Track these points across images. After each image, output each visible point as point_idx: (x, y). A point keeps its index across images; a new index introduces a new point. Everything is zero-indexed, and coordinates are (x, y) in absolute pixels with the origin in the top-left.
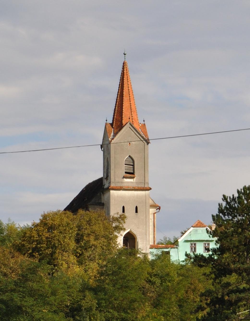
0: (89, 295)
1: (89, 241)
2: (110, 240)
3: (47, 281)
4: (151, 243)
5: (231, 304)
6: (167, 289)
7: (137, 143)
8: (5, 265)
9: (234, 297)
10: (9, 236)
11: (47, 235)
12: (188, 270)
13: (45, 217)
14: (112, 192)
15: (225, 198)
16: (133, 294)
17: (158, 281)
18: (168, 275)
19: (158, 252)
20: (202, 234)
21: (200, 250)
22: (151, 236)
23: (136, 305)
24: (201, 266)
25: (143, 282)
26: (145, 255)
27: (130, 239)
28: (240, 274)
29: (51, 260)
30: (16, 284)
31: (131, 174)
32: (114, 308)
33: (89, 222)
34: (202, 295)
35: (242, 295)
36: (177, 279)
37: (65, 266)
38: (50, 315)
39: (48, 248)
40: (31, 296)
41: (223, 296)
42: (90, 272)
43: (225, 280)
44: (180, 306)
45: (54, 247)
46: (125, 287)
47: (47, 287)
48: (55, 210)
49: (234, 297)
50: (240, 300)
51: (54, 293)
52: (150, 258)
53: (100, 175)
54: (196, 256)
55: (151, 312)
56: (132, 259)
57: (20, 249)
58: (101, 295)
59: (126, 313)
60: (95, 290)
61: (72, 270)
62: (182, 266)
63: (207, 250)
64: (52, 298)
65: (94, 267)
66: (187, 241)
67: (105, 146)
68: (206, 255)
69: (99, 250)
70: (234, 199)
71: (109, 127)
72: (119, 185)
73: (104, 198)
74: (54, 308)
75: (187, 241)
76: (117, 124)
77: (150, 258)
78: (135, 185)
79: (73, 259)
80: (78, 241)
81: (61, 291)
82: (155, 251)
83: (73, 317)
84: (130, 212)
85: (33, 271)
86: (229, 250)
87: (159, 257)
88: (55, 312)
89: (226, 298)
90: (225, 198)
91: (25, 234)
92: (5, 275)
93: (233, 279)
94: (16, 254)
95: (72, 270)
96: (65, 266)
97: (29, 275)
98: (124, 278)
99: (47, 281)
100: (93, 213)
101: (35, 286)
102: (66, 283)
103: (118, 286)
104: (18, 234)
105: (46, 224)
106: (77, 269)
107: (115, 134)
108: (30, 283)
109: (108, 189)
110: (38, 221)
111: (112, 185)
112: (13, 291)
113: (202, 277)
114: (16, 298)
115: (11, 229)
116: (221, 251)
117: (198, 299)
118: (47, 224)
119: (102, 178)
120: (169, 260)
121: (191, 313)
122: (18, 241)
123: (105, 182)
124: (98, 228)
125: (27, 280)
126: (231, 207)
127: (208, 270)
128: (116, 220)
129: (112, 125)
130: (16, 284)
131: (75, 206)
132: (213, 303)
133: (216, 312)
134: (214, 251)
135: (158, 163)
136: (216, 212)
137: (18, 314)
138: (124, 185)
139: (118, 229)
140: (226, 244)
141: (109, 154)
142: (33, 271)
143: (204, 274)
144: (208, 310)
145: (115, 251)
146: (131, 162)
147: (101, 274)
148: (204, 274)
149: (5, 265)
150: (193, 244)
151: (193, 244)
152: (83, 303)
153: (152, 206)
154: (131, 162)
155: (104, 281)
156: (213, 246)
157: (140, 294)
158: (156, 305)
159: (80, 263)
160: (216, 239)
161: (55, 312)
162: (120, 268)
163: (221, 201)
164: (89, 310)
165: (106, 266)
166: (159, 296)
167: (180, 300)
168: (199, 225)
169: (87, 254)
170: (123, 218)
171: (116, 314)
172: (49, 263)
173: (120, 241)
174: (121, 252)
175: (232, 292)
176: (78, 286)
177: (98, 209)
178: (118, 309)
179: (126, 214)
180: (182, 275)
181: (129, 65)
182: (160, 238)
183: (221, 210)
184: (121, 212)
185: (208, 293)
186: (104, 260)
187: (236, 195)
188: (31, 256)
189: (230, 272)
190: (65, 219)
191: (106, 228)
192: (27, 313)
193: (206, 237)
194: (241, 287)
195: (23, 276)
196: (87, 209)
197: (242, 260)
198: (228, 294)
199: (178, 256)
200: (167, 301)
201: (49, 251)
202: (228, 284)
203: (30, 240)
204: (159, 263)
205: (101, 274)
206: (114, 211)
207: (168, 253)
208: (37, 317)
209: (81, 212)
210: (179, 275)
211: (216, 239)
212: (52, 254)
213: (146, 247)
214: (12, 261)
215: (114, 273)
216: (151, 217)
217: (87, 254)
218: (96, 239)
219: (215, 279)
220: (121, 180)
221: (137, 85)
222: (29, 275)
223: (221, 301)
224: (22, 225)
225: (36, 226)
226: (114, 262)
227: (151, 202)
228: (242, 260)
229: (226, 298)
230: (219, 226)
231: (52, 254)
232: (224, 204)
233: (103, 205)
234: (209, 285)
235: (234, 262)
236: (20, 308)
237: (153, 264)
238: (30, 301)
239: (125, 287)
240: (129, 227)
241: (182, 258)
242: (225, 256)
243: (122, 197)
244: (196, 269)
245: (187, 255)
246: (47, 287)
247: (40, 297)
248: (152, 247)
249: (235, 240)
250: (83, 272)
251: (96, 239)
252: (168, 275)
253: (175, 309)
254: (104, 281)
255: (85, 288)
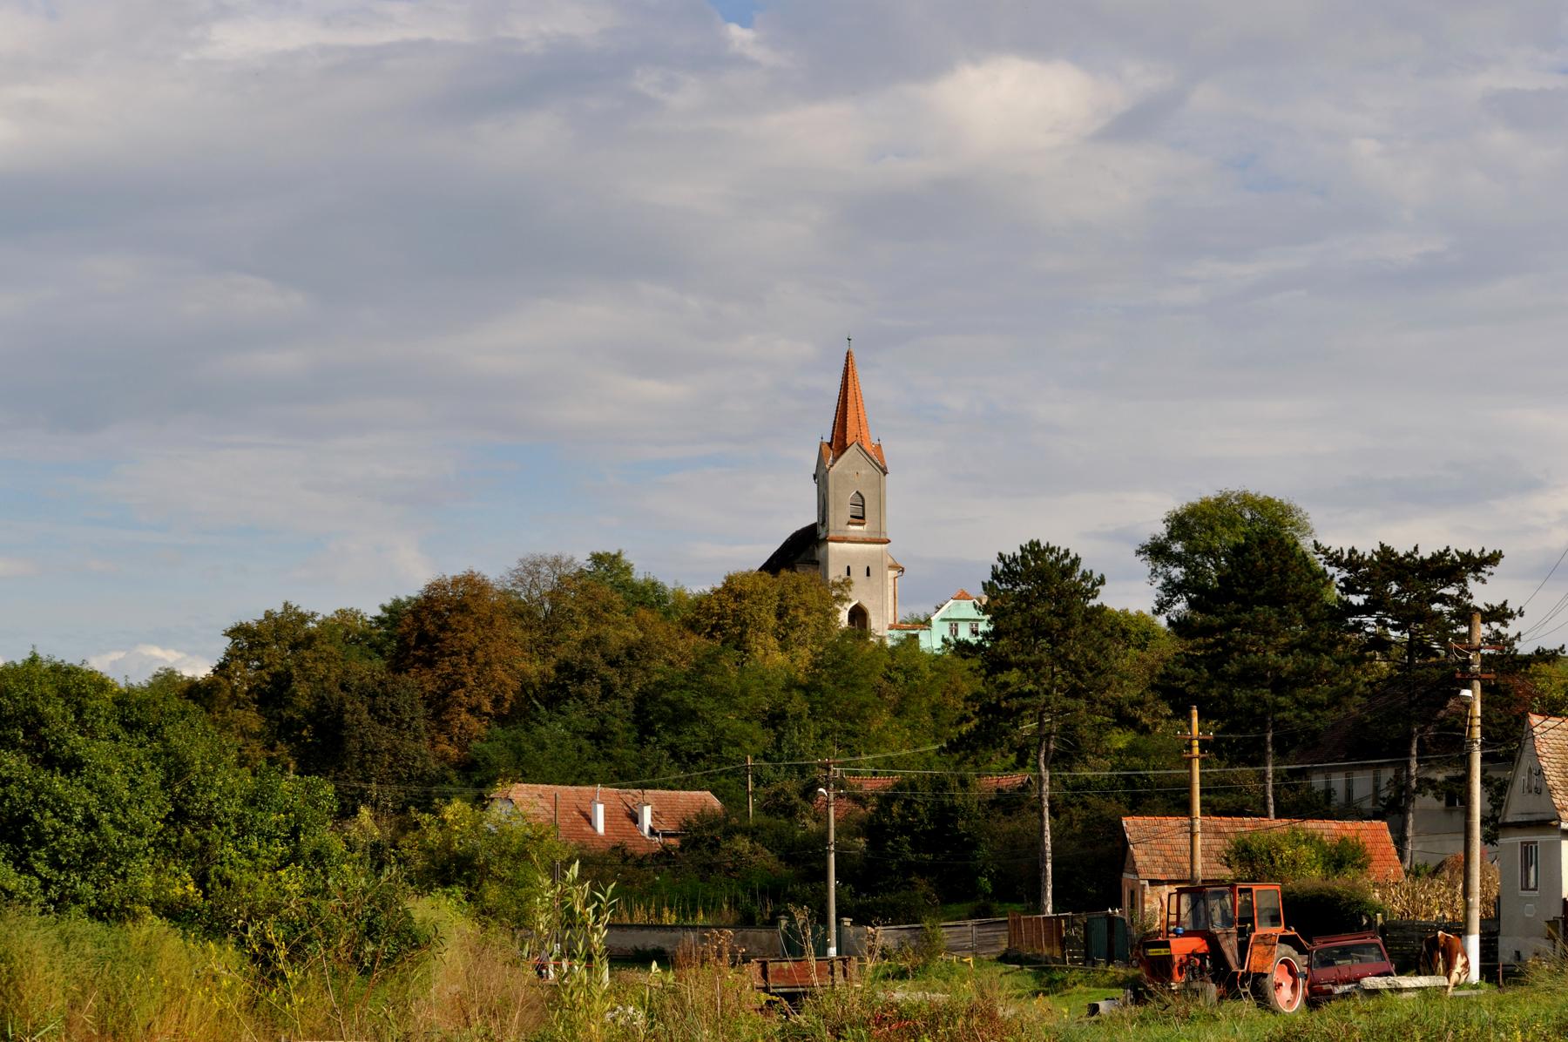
0: (797, 696)
1: (796, 617)
2: (829, 615)
3: (734, 674)
4: (891, 622)
5: (1009, 714)
6: (915, 689)
7: (867, 470)
8: (670, 649)
9: (1015, 703)
10: (675, 606)
11: (734, 606)
12: (947, 662)
13: (730, 579)
14: (831, 544)
15: (1001, 557)
16: (864, 696)
17: (901, 678)
18: (916, 669)
19: (902, 635)
20: (967, 610)
21: (964, 633)
22: (891, 612)
23: (868, 712)
24: (965, 657)
25: (877, 679)
26: (882, 639)
27: (858, 615)
28: (1024, 670)
29: (741, 644)
30: (687, 677)
31: (859, 519)
32: (834, 715)
33: (797, 589)
34: (967, 699)
35: (1028, 701)
36: (929, 675)
37: (761, 652)
38: (739, 724)
39: (735, 626)
40: (710, 695)
41: (998, 702)
42: (798, 661)
43: (1002, 678)
44: (934, 715)
45: (744, 624)
46: (851, 686)
47: (734, 683)
48: (745, 569)
49: (1015, 703)
50: (1024, 707)
51: (744, 692)
52: (889, 643)
53: (812, 518)
54: (958, 642)
55: (892, 722)
56: (861, 644)
57: (692, 626)
58: (816, 696)
59: (853, 723)
60: (806, 689)
61: (770, 658)
62: (938, 657)
63: (975, 633)
64: (742, 699)
65: (804, 655)
66: (944, 620)
67: (821, 477)
68: (973, 640)
69: (812, 630)
70: (1015, 559)
71: (826, 449)
72: (841, 534)
73: (819, 554)
74: (746, 714)
75: (944, 620)
76: (838, 443)
77: (889, 643)
78: (866, 536)
79: (772, 642)
80: (780, 616)
81: (755, 689)
82: (896, 633)
83: (774, 727)
84: (858, 575)
85: (713, 658)
86: (1007, 634)
87: (902, 643)
88: (746, 719)
89: (1004, 704)
90: (1001, 557)
91: (700, 604)
92: (671, 663)
93: (1013, 676)
94: (688, 633)
95: (770, 658)
96: (761, 652)
97: (708, 665)
98: (850, 671)
99: (734, 674)
100: (802, 575)
101: (716, 680)
102: (762, 677)
103: (841, 683)
104: (689, 604)
105: (731, 590)
106: (779, 658)
107: (836, 459)
108: (709, 677)
109: (825, 541)
110: (719, 586)
111: (832, 535)
112: (682, 687)
113: (967, 674)
114: (689, 698)
115: (679, 595)
116: (996, 635)
117: (961, 706)
118: (733, 589)
119: (814, 526)
120: (917, 647)
121: (951, 725)
122: (690, 615)
123: (820, 529)
124: (810, 597)
125: (704, 672)
126: (1011, 571)
127: (976, 663)
128: (838, 586)
129: (830, 445)
130: (687, 677)
131: (774, 565)
132: (984, 710)
133: (989, 724)
134: (985, 635)
135: (900, 504)
136: (988, 578)
137: (691, 720)
138: (850, 535)
139: (841, 599)
140: (1004, 625)
141: (827, 488)
142: (713, 658)
143: (971, 669)
144: (976, 721)
145: (835, 632)
146: (860, 501)
147: (816, 665)
148: (971, 669)
149: (670, 649)
150: (954, 624)
151: (954, 624)
152: (788, 707)
153: (892, 567)
154: (860, 501)
155: (819, 676)
156: (983, 627)
157: (873, 697)
158: (898, 712)
159: (784, 649)
160: (988, 617)
161: (746, 719)
162: (844, 657)
163: (996, 562)
164: (798, 717)
165: (822, 654)
166: (903, 699)
167: (934, 707)
168: (963, 596)
169: (794, 636)
170: (847, 583)
171: (838, 724)
172: (737, 648)
173: (844, 617)
174: (844, 634)
175: (1012, 695)
176: (781, 682)
177: (810, 569)
178: (841, 717)
179: (853, 577)
180: (938, 670)
181: (856, 356)
182: (903, 614)
183: (995, 576)
184: (844, 575)
185: (976, 697)
186: (820, 644)
187: (1019, 553)
188: (710, 636)
189: (1008, 666)
190: (761, 584)
191: (822, 598)
192: (704, 720)
193: (973, 614)
194: (1026, 689)
195: (698, 666)
196: (793, 569)
197: (1027, 649)
198: (1006, 699)
199: (931, 641)
200: (914, 708)
201: (737, 630)
202: (1006, 685)
203: (708, 613)
204: (902, 651)
205: (816, 665)
206: (835, 573)
207: (916, 636)
208: (720, 726)
209: (784, 573)
210: (932, 669)
211: (988, 617)
212: (741, 635)
213: (882, 627)
214: (682, 643)
215: (835, 665)
216: (891, 582)
217: (794, 636)
218: (808, 614)
219: (986, 677)
220: (844, 527)
221: (868, 386)
222: (708, 665)
223: (995, 709)
224: (695, 591)
225: (717, 592)
226: (835, 648)
227: (890, 561)
228: (1027, 649)
229: (1004, 704)
230: (992, 598)
231: (741, 635)
232: (1000, 566)
233: (818, 564)
234: (978, 685)
235: (1015, 653)
236: (694, 712)
237: (893, 652)
238: (709, 703)
239: (851, 686)
240: (856, 597)
241: (938, 644)
242: (1002, 642)
243: (846, 553)
244: (958, 661)
245: (944, 640)
246: (734, 683)
247: (725, 697)
248: (891, 628)
249: (1017, 619)
250: (788, 662)
251: (808, 614)
252: (916, 669)
253: (926, 719)
254: (819, 676)
255: (792, 685)
